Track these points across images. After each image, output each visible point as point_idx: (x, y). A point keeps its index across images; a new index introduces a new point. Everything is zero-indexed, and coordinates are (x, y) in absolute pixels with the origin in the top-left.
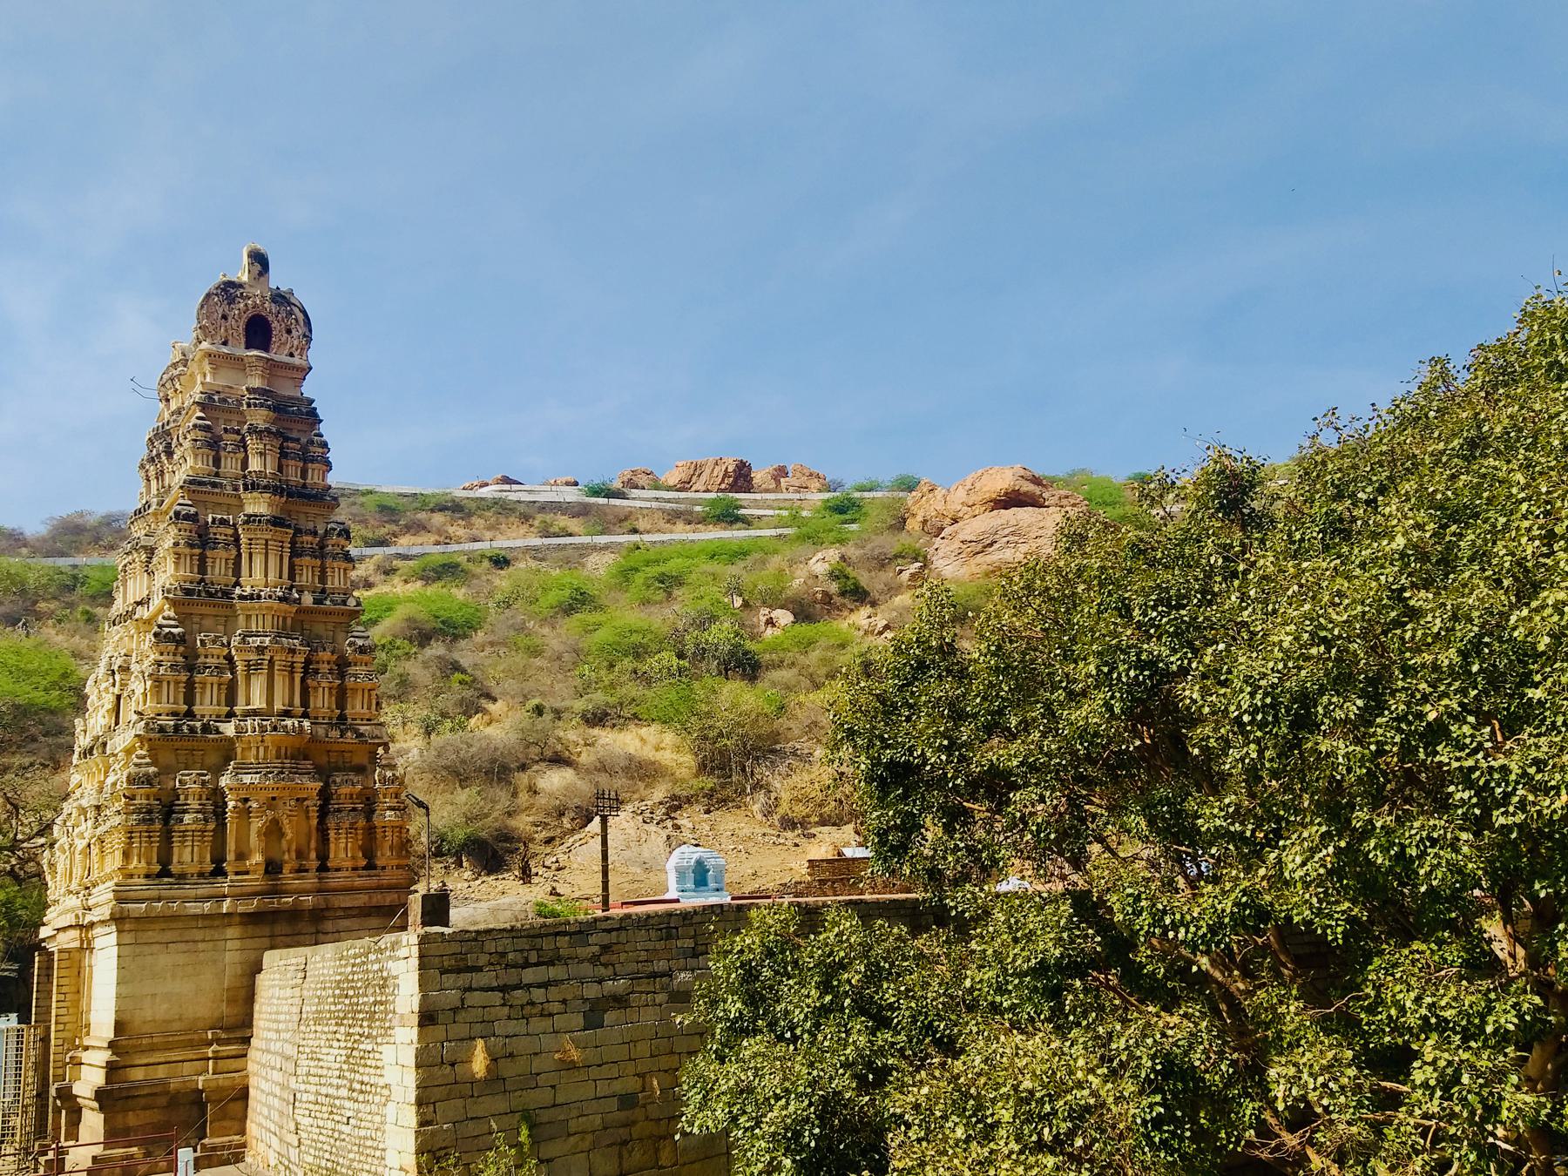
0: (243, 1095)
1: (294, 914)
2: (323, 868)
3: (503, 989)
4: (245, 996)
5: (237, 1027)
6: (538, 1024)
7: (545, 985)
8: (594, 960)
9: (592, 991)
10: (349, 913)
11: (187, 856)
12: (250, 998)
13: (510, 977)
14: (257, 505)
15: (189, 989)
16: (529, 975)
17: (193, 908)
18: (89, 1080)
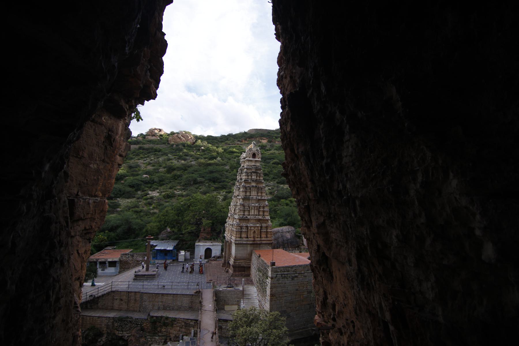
0: (250, 267)
1: (257, 244)
2: (261, 237)
3: (282, 275)
4: (251, 255)
5: (250, 259)
6: (286, 279)
7: (287, 274)
8: (293, 271)
9: (293, 275)
10: (264, 244)
11: (244, 235)
12: (251, 255)
13: (283, 273)
14: (254, 184)
15: (244, 252)
16: (285, 273)
17: (244, 242)
18: (232, 262)
